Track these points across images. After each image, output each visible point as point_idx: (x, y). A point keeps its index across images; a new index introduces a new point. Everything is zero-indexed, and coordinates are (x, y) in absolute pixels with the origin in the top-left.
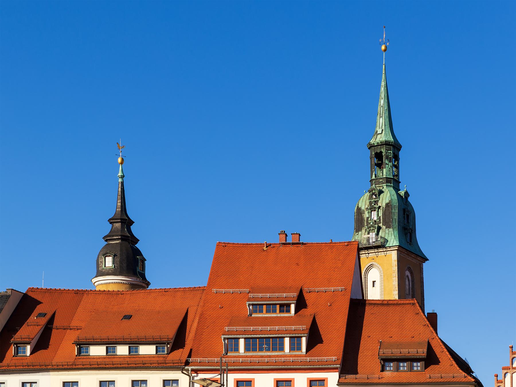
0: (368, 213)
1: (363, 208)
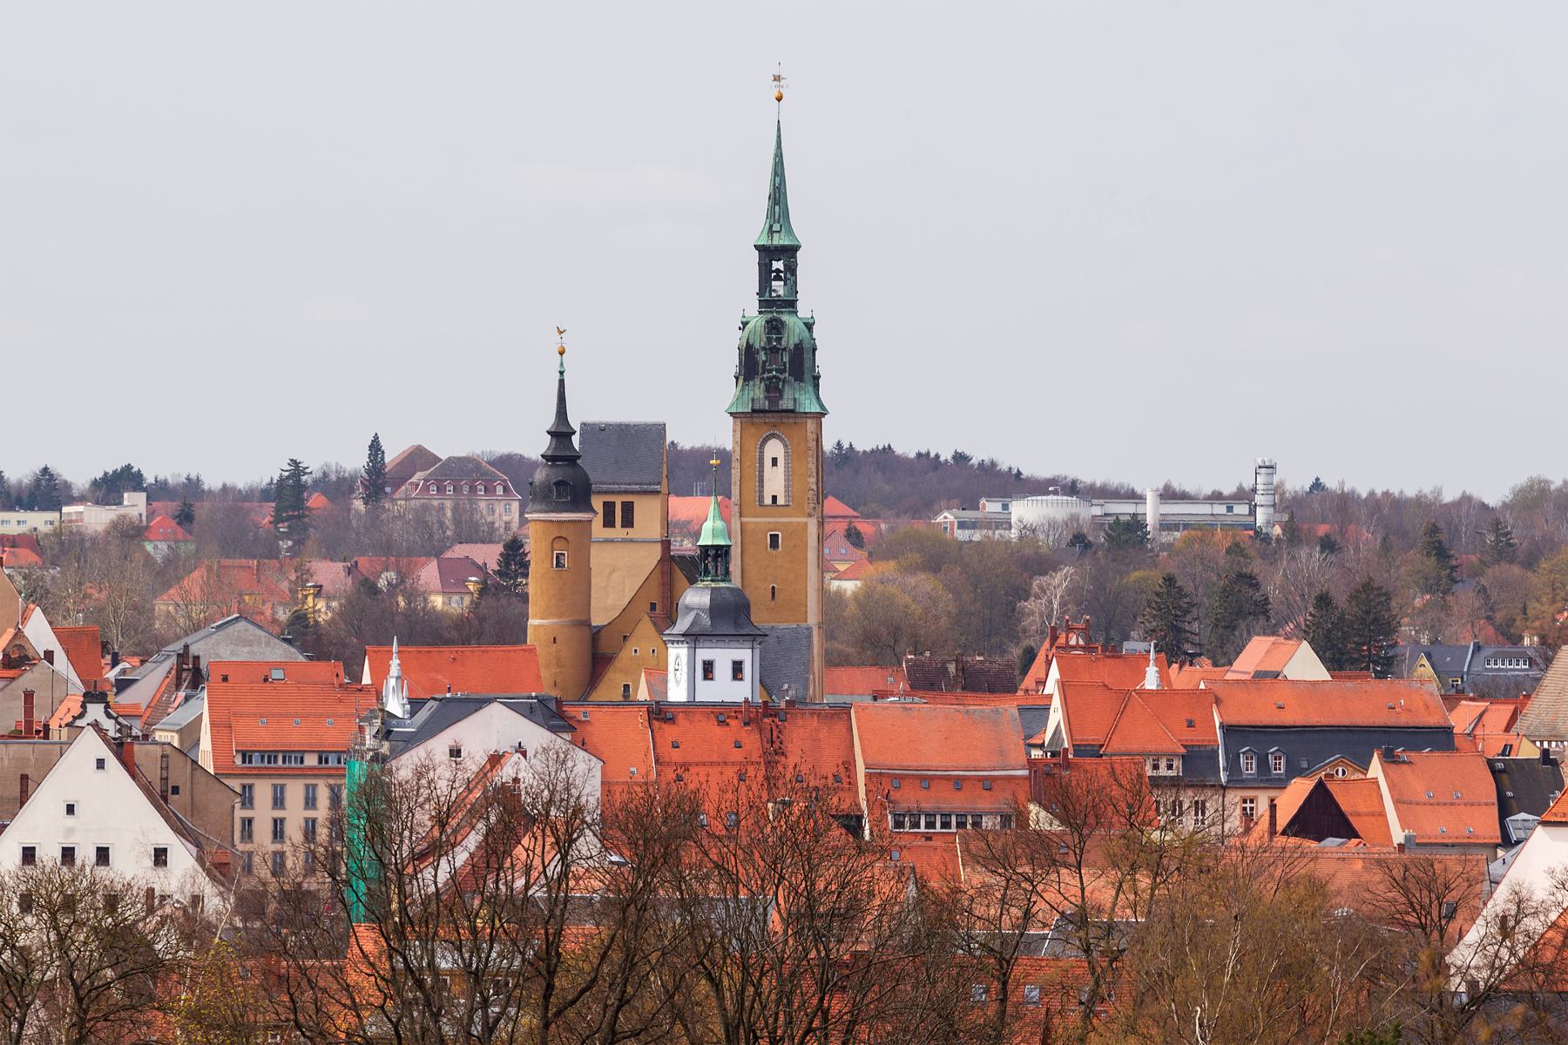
1: (757, 346)
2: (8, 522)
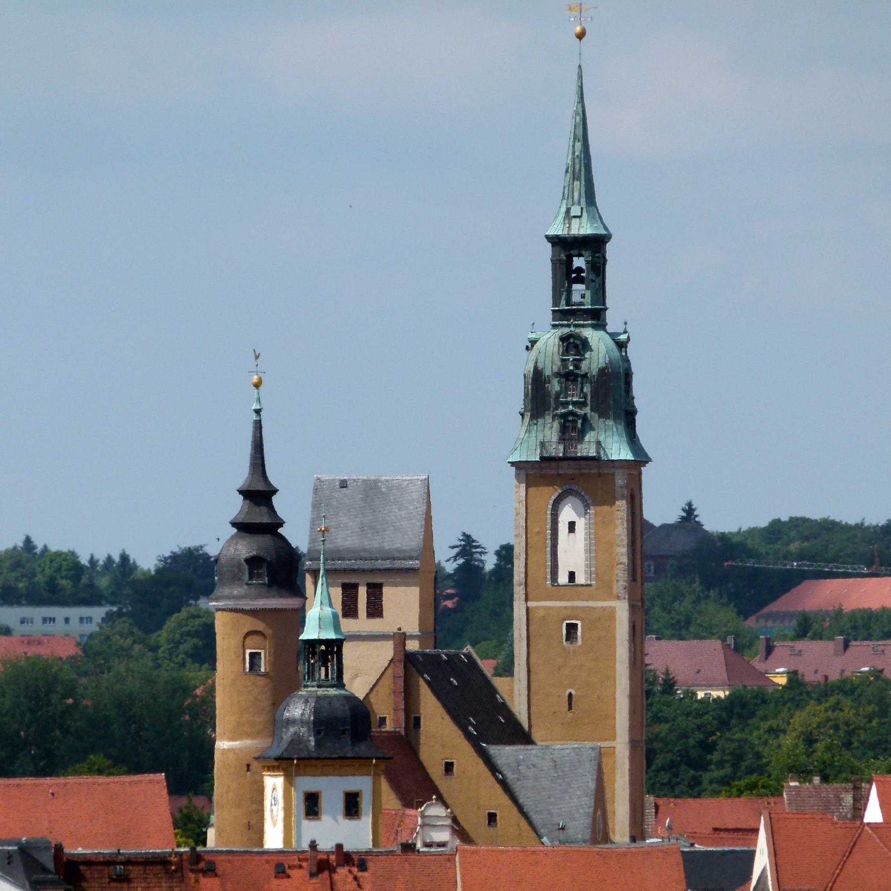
0: (559, 382)
1: (548, 372)
2: (52, 620)
